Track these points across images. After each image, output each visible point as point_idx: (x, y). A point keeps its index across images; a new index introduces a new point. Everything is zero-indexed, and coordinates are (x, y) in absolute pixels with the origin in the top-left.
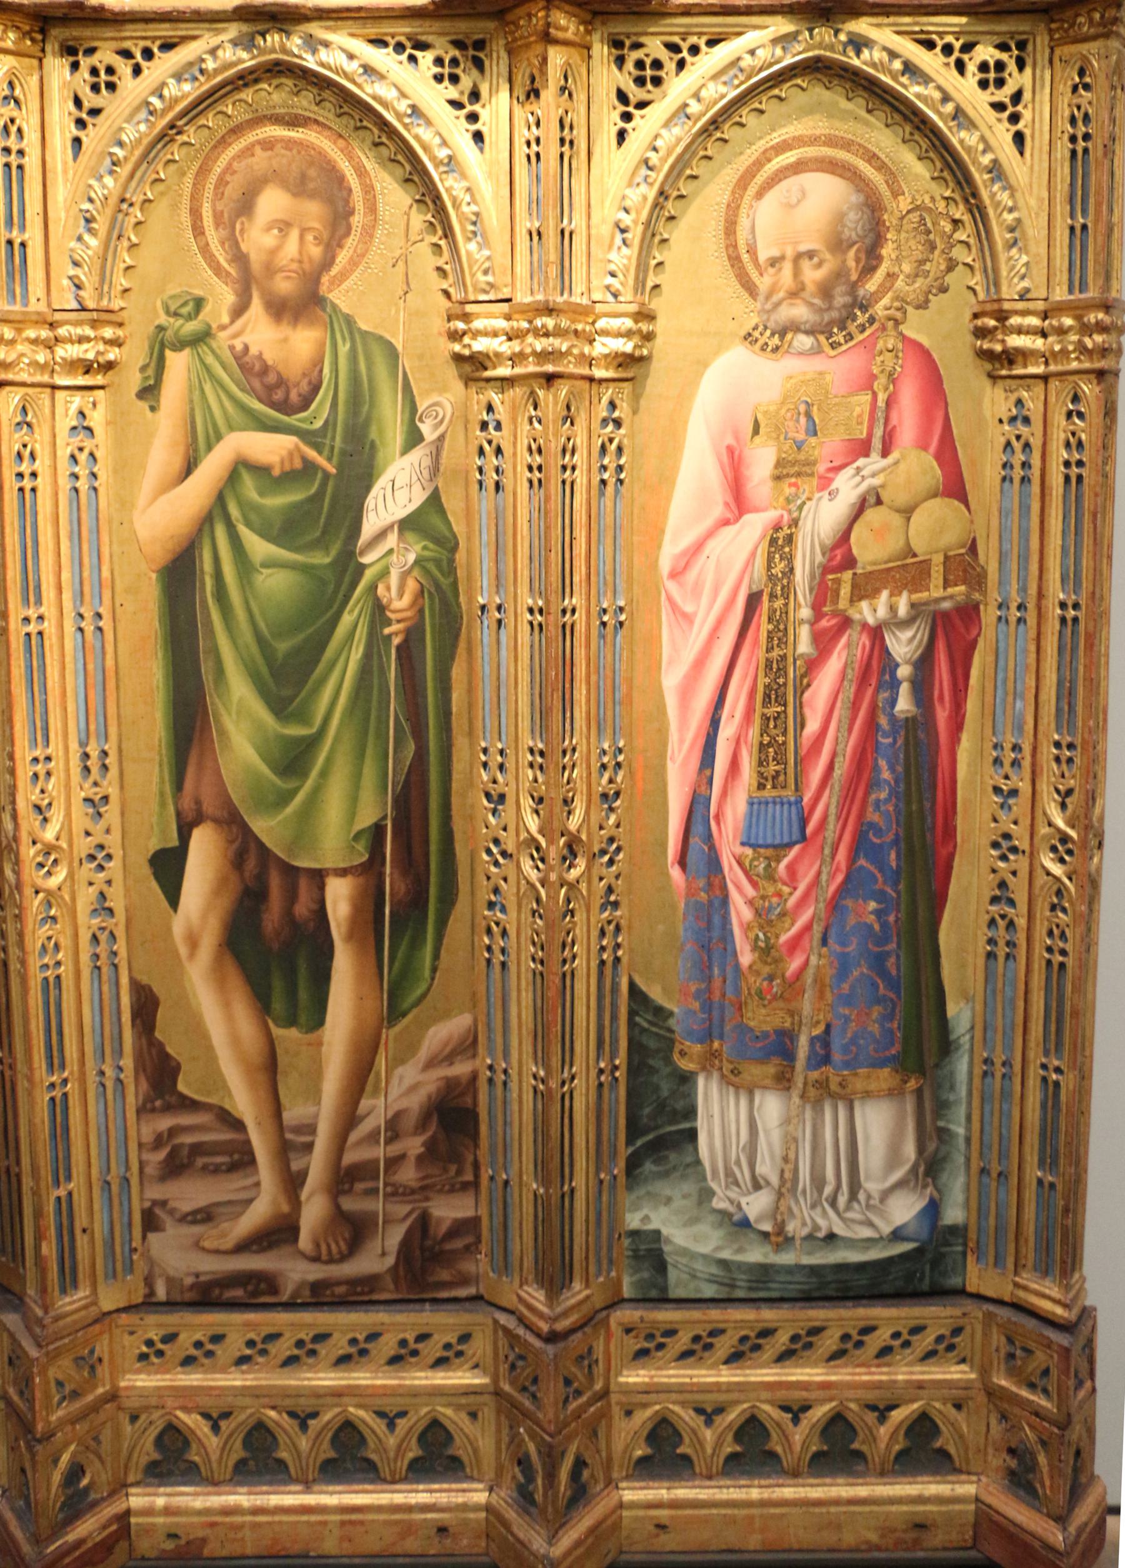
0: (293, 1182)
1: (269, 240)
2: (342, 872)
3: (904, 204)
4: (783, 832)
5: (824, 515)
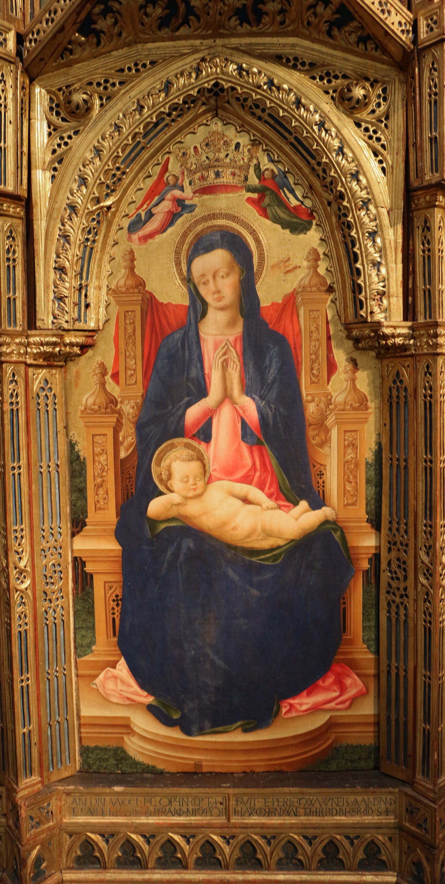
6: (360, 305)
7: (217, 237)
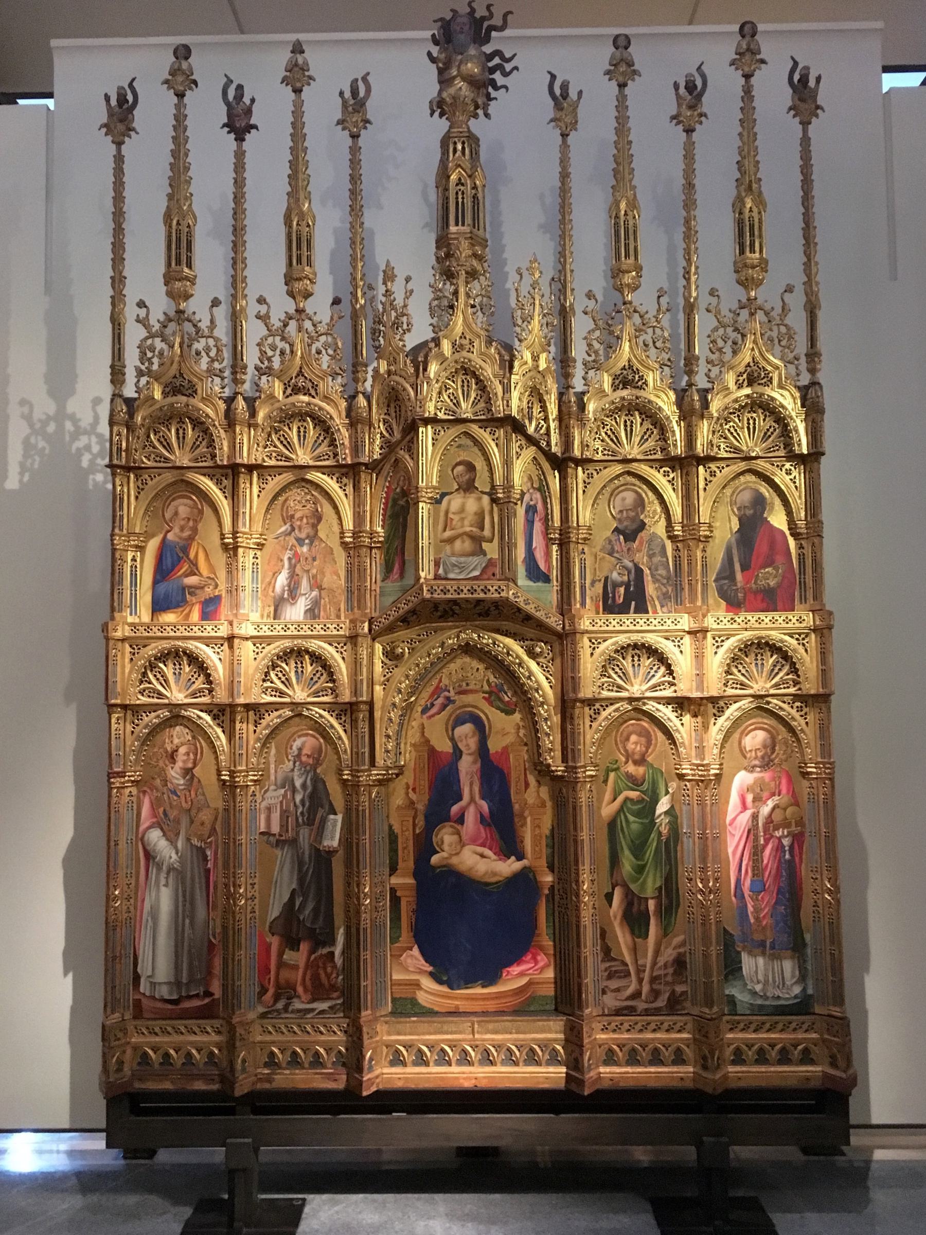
0: (640, 981)
1: (633, 746)
2: (652, 898)
3: (780, 737)
4: (759, 888)
5: (766, 810)
6: (540, 755)
7: (467, 717)
